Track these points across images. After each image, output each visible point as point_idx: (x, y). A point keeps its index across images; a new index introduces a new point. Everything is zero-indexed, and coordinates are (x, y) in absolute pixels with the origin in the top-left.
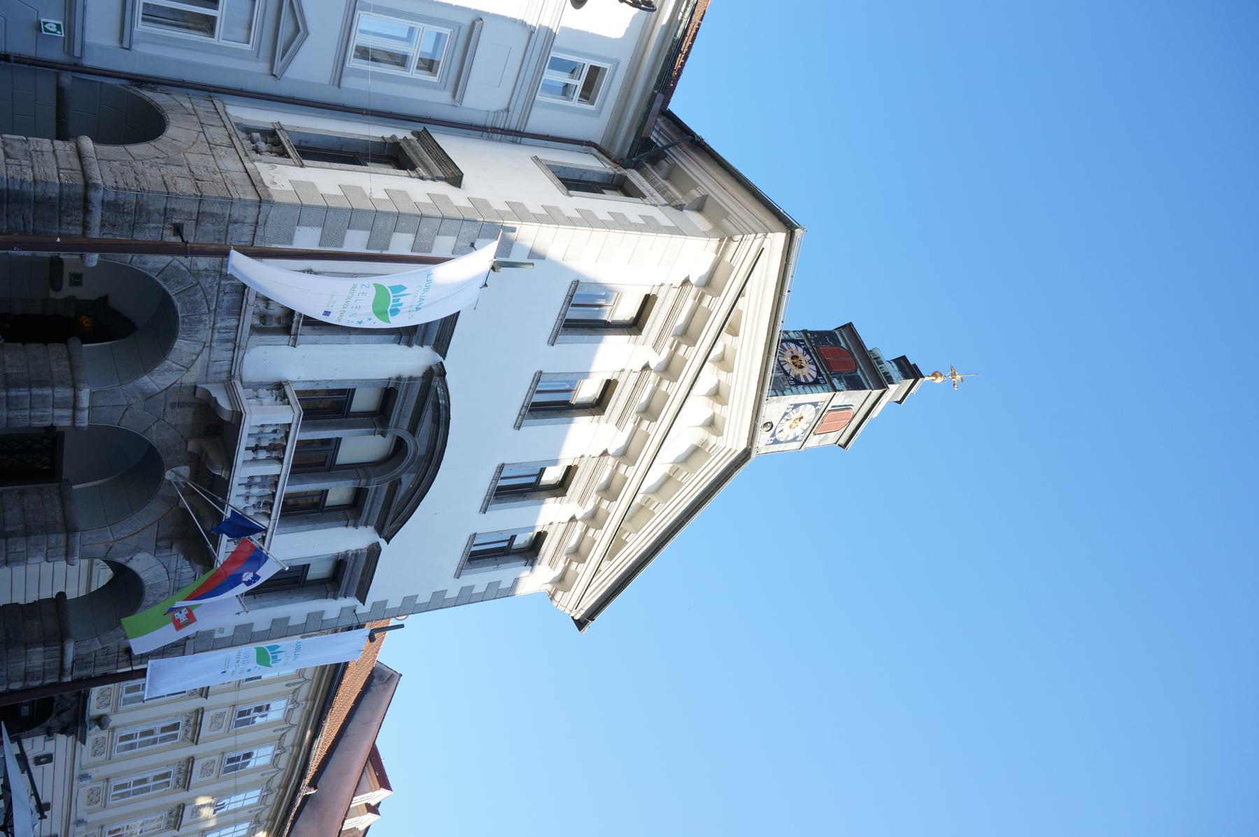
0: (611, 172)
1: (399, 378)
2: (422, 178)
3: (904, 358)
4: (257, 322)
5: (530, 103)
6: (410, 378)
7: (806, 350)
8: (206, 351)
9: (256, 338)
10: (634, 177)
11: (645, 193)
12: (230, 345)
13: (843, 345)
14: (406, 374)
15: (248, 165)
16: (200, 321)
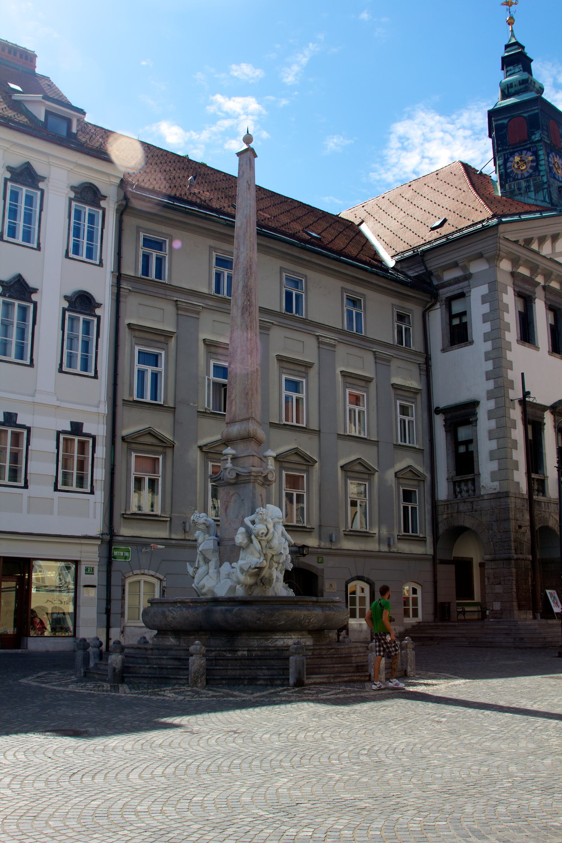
0: (444, 306)
1: (555, 427)
2: (477, 420)
3: (503, 58)
4: (541, 494)
5: (416, 353)
6: (555, 421)
7: (512, 154)
8: (552, 514)
9: (547, 495)
10: (445, 293)
11: (460, 291)
12: (549, 504)
13: (505, 121)
14: (553, 424)
15: (486, 497)
16: (543, 517)
